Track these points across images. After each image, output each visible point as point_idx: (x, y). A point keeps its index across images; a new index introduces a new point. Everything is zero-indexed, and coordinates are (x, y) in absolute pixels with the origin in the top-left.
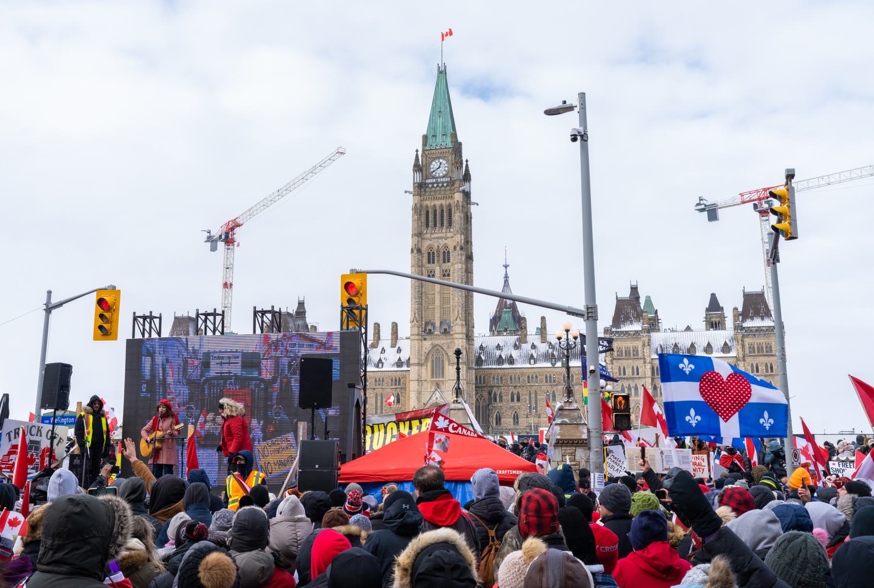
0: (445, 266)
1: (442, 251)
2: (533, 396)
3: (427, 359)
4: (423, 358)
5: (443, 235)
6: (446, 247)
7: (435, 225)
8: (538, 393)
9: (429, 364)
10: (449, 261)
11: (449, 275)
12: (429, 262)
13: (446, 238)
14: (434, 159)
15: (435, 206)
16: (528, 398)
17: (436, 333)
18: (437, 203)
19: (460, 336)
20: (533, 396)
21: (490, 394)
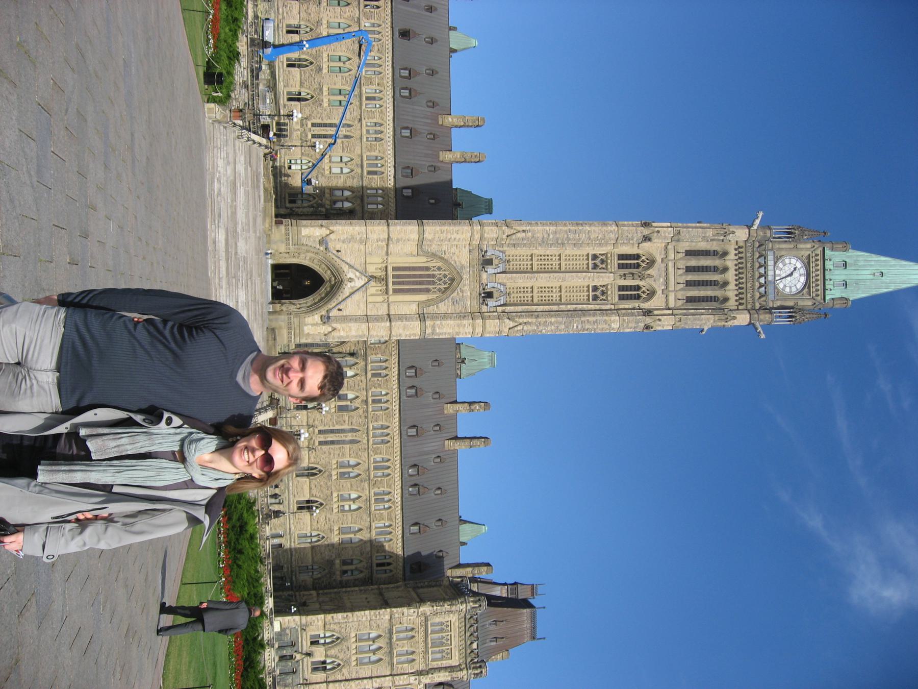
0: (613, 295)
1: (641, 283)
2: (350, 437)
3: (434, 255)
4: (434, 248)
5: (672, 288)
6: (652, 294)
7: (689, 269)
8: (355, 446)
9: (421, 261)
10: (622, 298)
11: (595, 298)
12: (621, 257)
13: (666, 291)
14: (807, 266)
15: (725, 269)
16: (346, 427)
17: (484, 276)
18: (731, 276)
19: (479, 330)
20: (350, 437)
21: (352, 354)
